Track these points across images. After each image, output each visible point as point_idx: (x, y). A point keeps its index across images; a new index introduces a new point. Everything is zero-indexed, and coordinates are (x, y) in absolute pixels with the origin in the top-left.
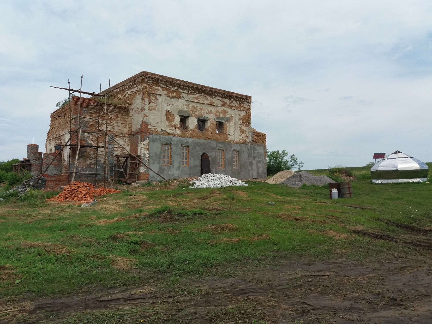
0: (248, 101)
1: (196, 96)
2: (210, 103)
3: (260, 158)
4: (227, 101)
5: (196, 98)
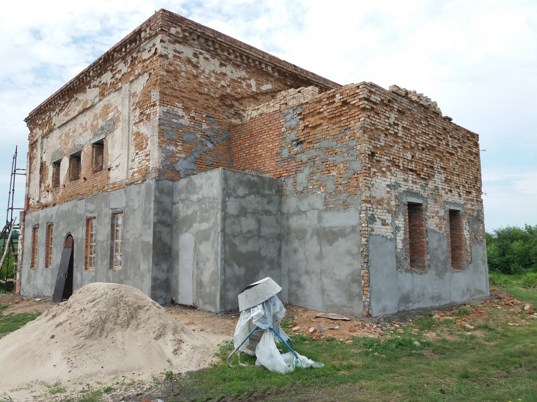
0: (143, 34)
1: (66, 110)
2: (82, 109)
3: (206, 220)
4: (107, 77)
5: (66, 115)
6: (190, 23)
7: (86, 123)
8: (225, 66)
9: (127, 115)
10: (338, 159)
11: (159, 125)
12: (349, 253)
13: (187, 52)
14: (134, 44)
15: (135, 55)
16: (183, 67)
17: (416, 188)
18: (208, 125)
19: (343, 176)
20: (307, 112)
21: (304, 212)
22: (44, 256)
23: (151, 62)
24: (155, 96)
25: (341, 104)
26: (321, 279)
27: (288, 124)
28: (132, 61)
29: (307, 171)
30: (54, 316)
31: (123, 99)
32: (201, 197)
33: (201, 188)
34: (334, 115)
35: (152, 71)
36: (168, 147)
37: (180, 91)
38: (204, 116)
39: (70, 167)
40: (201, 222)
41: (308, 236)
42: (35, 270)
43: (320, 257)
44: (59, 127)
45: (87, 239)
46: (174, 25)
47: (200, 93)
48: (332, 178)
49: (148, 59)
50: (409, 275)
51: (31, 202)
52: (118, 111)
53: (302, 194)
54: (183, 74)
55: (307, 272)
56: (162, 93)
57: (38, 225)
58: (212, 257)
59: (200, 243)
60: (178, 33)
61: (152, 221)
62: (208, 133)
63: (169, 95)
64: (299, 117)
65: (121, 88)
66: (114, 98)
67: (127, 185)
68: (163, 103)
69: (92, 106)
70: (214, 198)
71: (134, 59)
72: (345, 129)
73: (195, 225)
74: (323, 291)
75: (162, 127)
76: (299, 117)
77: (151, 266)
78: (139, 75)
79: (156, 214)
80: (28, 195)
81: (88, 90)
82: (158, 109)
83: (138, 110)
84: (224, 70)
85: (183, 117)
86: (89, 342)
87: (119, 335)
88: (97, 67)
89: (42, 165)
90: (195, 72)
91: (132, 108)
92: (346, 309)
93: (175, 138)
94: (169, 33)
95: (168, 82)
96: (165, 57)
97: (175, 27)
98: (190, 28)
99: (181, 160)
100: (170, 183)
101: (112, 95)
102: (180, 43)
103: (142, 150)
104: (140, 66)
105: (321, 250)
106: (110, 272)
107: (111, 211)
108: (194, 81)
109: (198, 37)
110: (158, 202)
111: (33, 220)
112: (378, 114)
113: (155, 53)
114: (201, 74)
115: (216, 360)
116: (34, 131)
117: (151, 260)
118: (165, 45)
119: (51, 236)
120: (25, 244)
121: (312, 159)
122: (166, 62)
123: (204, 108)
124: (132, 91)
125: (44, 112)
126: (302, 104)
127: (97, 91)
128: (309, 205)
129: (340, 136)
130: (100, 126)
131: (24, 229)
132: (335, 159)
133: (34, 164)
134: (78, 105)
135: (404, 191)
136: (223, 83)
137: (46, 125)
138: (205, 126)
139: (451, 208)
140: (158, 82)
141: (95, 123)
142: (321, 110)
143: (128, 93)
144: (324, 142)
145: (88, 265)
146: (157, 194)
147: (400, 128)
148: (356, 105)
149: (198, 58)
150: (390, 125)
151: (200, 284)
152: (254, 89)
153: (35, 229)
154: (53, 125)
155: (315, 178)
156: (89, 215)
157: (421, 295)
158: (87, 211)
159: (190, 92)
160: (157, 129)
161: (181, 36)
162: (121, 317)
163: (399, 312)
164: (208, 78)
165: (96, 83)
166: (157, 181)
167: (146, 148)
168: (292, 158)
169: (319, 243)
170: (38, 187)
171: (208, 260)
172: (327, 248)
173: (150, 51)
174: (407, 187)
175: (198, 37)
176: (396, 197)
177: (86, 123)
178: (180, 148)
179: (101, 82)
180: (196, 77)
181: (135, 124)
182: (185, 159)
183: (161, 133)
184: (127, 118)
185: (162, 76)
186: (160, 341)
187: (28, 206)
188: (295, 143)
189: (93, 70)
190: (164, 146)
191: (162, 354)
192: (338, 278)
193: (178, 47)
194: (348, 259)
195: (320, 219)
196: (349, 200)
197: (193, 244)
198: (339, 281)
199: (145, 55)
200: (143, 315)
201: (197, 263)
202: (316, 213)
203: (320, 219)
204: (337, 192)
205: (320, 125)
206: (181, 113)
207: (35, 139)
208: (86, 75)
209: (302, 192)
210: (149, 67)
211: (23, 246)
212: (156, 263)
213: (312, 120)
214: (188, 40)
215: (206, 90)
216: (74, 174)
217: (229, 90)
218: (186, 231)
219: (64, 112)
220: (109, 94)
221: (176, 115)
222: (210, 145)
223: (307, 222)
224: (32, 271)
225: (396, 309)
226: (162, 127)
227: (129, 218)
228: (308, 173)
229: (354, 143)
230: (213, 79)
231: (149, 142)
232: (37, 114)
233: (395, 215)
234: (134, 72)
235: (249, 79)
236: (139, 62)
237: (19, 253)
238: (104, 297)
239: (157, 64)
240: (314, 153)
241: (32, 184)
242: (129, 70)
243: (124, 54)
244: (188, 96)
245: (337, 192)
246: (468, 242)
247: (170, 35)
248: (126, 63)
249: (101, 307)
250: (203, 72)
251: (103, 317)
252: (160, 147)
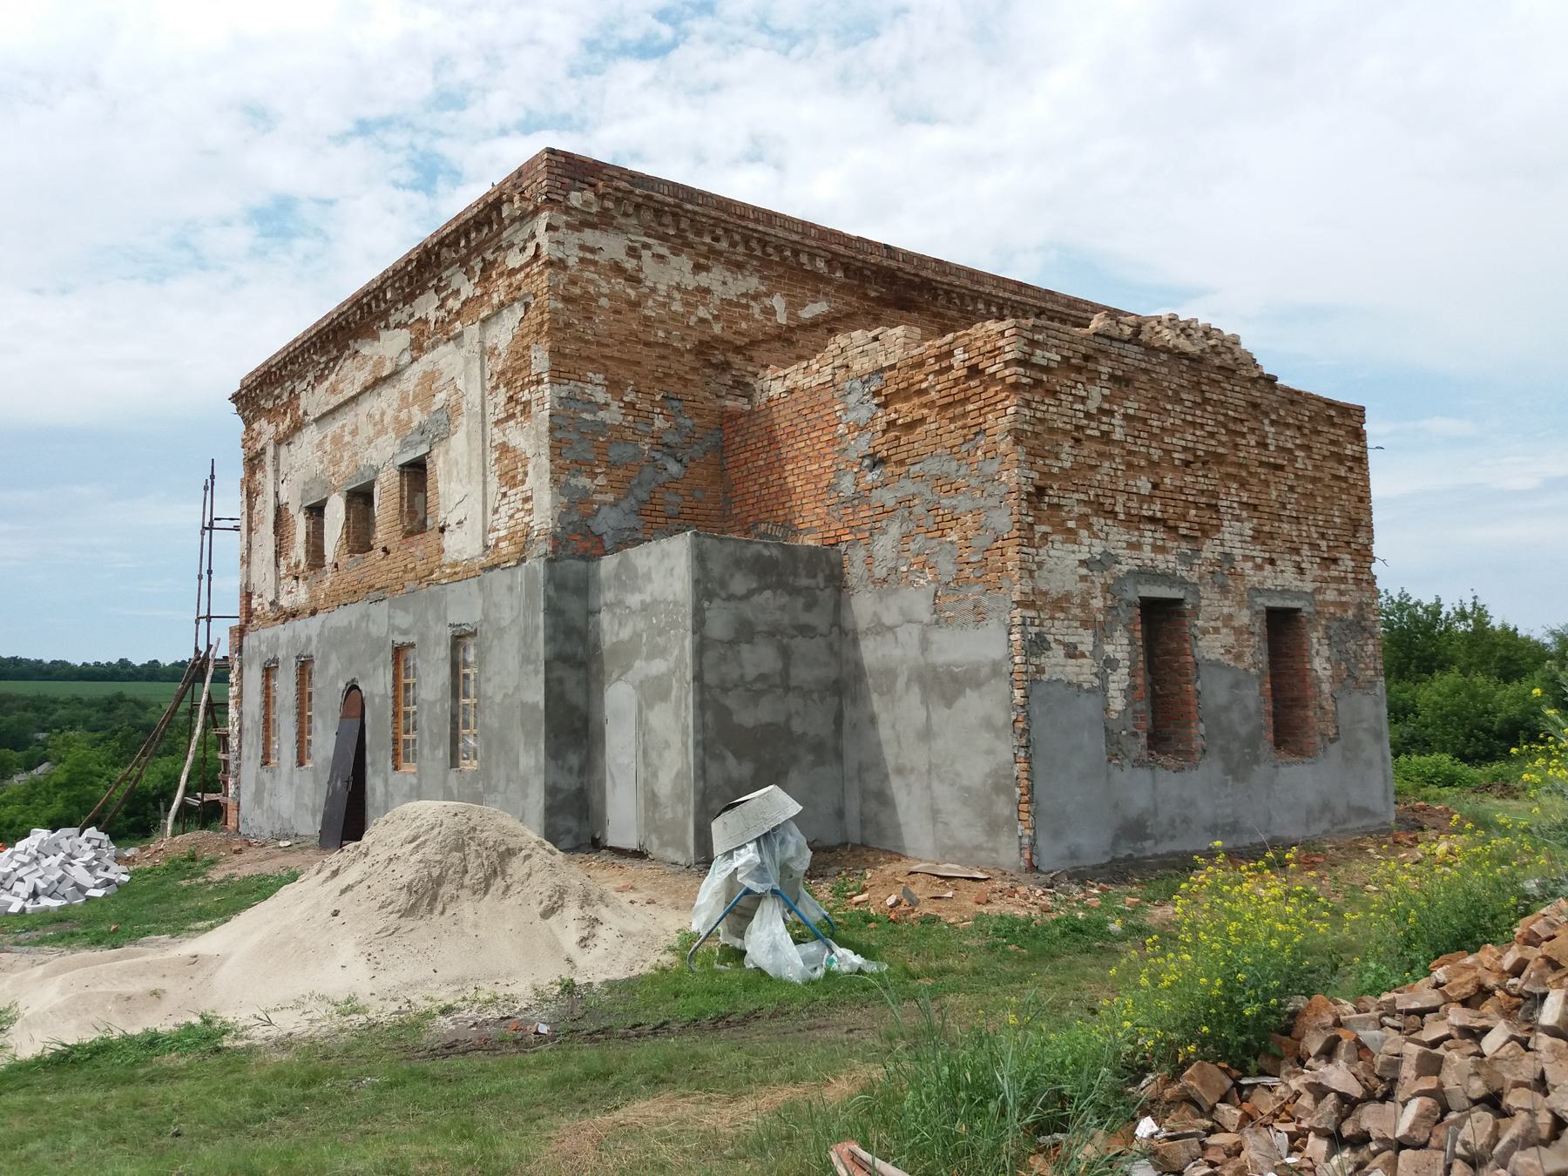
1: (332, 378)
2: (370, 379)
3: (662, 652)
4: (427, 306)
5: (333, 390)
6: (616, 174)
7: (383, 414)
8: (707, 269)
9: (478, 401)
10: (963, 503)
11: (551, 430)
12: (988, 724)
13: (612, 246)
14: (486, 230)
15: (489, 256)
16: (603, 283)
17: (1164, 562)
18: (667, 418)
19: (974, 543)
20: (893, 388)
21: (891, 629)
22: (294, 738)
23: (527, 276)
24: (540, 360)
25: (964, 372)
26: (929, 787)
27: (852, 416)
28: (482, 270)
29: (895, 530)
30: (335, 873)
31: (467, 361)
32: (648, 600)
33: (648, 577)
34: (950, 399)
35: (530, 299)
36: (573, 481)
37: (599, 344)
38: (658, 398)
39: (347, 519)
40: (650, 657)
41: (901, 683)
42: (272, 770)
43: (927, 734)
44: (316, 421)
45: (395, 698)
46: (578, 184)
47: (647, 344)
48: (948, 547)
49: (521, 268)
50: (1143, 774)
51: (254, 604)
52: (457, 391)
53: (885, 584)
54: (604, 302)
55: (900, 771)
56: (555, 353)
57: (275, 660)
58: (676, 739)
59: (650, 706)
60: (586, 203)
61: (542, 657)
62: (668, 438)
63: (572, 357)
64: (875, 401)
65: (461, 334)
66: (445, 358)
67: (484, 569)
68: (557, 376)
69: (396, 373)
70: (676, 603)
71: (487, 266)
72: (976, 434)
73: (638, 664)
74: (935, 814)
75: (558, 435)
76: (875, 401)
77: (542, 760)
78: (502, 305)
79: (549, 639)
80: (247, 586)
81: (384, 334)
82: (547, 392)
83: (503, 390)
84: (703, 279)
85: (607, 404)
86: (407, 923)
87: (467, 908)
88: (401, 279)
89: (280, 511)
90: (632, 293)
91: (488, 385)
92: (983, 854)
93: (590, 456)
94: (568, 208)
95: (568, 325)
96: (557, 265)
97: (581, 190)
98: (617, 189)
99: (605, 509)
100: (581, 565)
101: (442, 349)
102: (593, 226)
103: (515, 485)
104: (503, 283)
105: (928, 717)
106: (453, 774)
107: (449, 632)
108: (631, 315)
109: (638, 206)
110: (552, 610)
111: (264, 648)
112: (1054, 394)
113: (536, 256)
114: (646, 296)
115: (668, 959)
116: (256, 426)
117: (542, 746)
118: (558, 235)
119: (308, 690)
120: (245, 708)
121: (905, 503)
122: (563, 277)
123: (658, 380)
124: (488, 344)
125: (280, 381)
126: (882, 370)
127: (402, 337)
128: (902, 611)
129: (964, 448)
130: (415, 424)
131: (241, 670)
132: (954, 502)
133: (257, 507)
134: (359, 369)
135: (1129, 572)
136: (702, 312)
137: (285, 413)
138: (659, 423)
139: (1271, 604)
140: (546, 327)
141: (403, 415)
142: (924, 385)
143: (477, 349)
144: (930, 461)
145: (401, 758)
146: (552, 593)
147: (1117, 421)
148: (999, 376)
149: (640, 257)
150: (1088, 415)
151: (651, 801)
152: (782, 319)
153: (269, 671)
154: (301, 412)
155: (912, 546)
156: (399, 640)
157: (1178, 821)
158: (393, 628)
159: (621, 343)
160: (546, 440)
161: (594, 209)
162: (471, 871)
163: (1114, 860)
164: (664, 305)
165: (403, 317)
166: (550, 562)
167: (523, 482)
168: (861, 497)
169: (925, 702)
170: (273, 568)
171: (667, 745)
172: (940, 714)
173: (523, 250)
174: (1139, 562)
175: (638, 206)
176: (1107, 589)
177: (383, 414)
178: (601, 480)
179: (412, 315)
180: (635, 305)
181: (497, 423)
182: (615, 505)
183: (556, 449)
184: (478, 409)
185: (554, 312)
186: (553, 920)
187: (249, 613)
188: (867, 462)
189: (392, 285)
190: (563, 478)
191: (555, 947)
192: (965, 782)
193: (590, 237)
194: (985, 739)
195: (925, 644)
196: (985, 601)
197: (634, 710)
198: (968, 789)
199: (514, 260)
200: (516, 867)
201: (645, 752)
202: (915, 630)
203: (925, 644)
204: (960, 582)
205: (922, 420)
206: (601, 396)
207: (259, 447)
208: (376, 298)
209: (885, 581)
210: (524, 290)
211: (241, 714)
212: (554, 753)
213: (904, 407)
214: (614, 218)
215: (661, 334)
216: (357, 538)
217: (717, 329)
218: (618, 679)
219: (326, 384)
220: (434, 347)
221: (590, 402)
222: (674, 468)
223: (898, 652)
224: (266, 776)
225: (1106, 853)
226: (558, 435)
227: (490, 648)
228: (898, 536)
229: (995, 466)
230: (677, 307)
231: (530, 468)
232: (260, 385)
233: (1102, 632)
234: (490, 296)
235: (769, 295)
236: (501, 275)
237: (233, 729)
238: (436, 831)
239: (542, 283)
240: (909, 487)
241: (255, 558)
242: (478, 292)
243: (464, 251)
244: (617, 354)
245: (960, 582)
246: (1326, 687)
247: (568, 210)
248: (469, 273)
249: (429, 851)
250: (653, 290)
251: (436, 872)
252: (555, 481)
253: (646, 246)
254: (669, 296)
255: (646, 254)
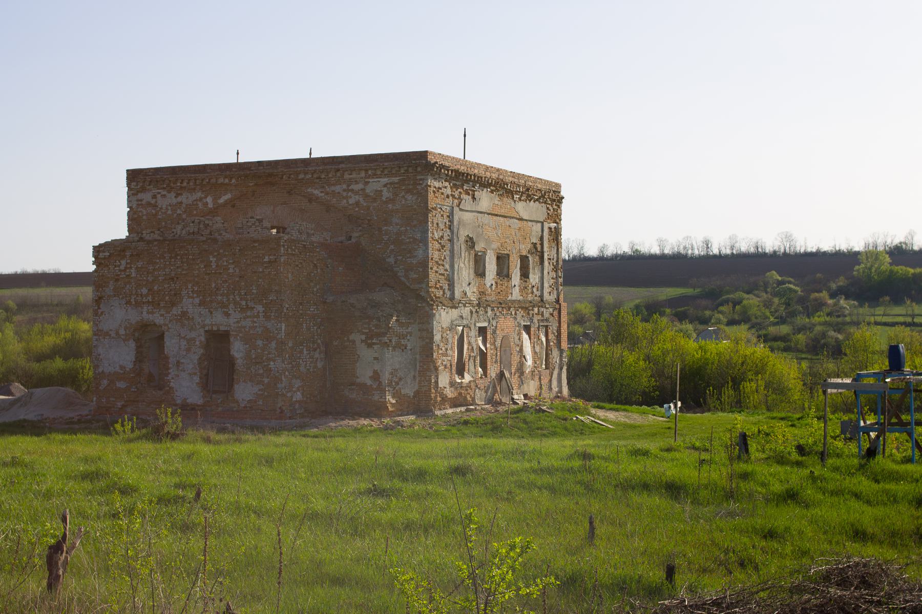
8: (181, 194)
54: (144, 217)
84: (179, 199)
102: (141, 192)
136: (179, 212)
147: (133, 271)
150: (120, 271)
152: (210, 206)
230: (169, 212)
235: (206, 197)
250: (161, 208)
253: (159, 193)
254: (167, 209)
255: (159, 196)
